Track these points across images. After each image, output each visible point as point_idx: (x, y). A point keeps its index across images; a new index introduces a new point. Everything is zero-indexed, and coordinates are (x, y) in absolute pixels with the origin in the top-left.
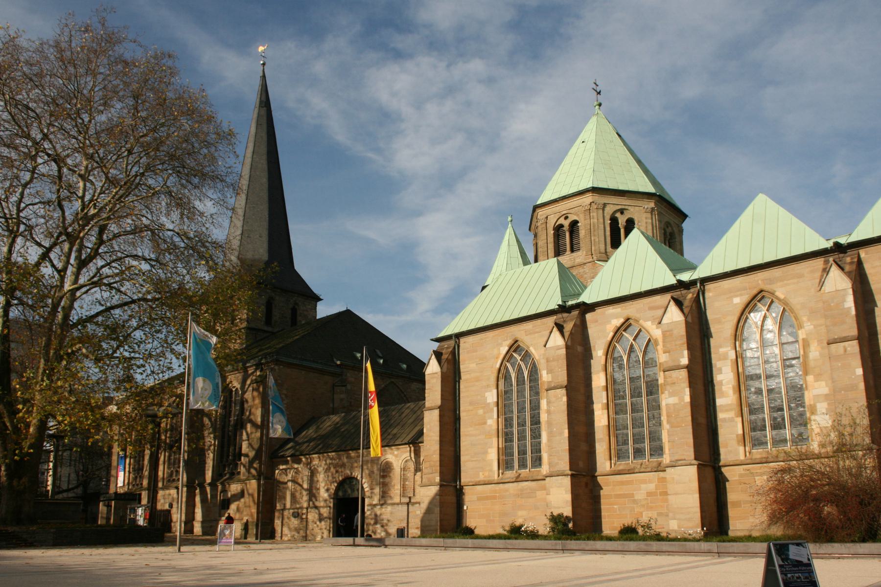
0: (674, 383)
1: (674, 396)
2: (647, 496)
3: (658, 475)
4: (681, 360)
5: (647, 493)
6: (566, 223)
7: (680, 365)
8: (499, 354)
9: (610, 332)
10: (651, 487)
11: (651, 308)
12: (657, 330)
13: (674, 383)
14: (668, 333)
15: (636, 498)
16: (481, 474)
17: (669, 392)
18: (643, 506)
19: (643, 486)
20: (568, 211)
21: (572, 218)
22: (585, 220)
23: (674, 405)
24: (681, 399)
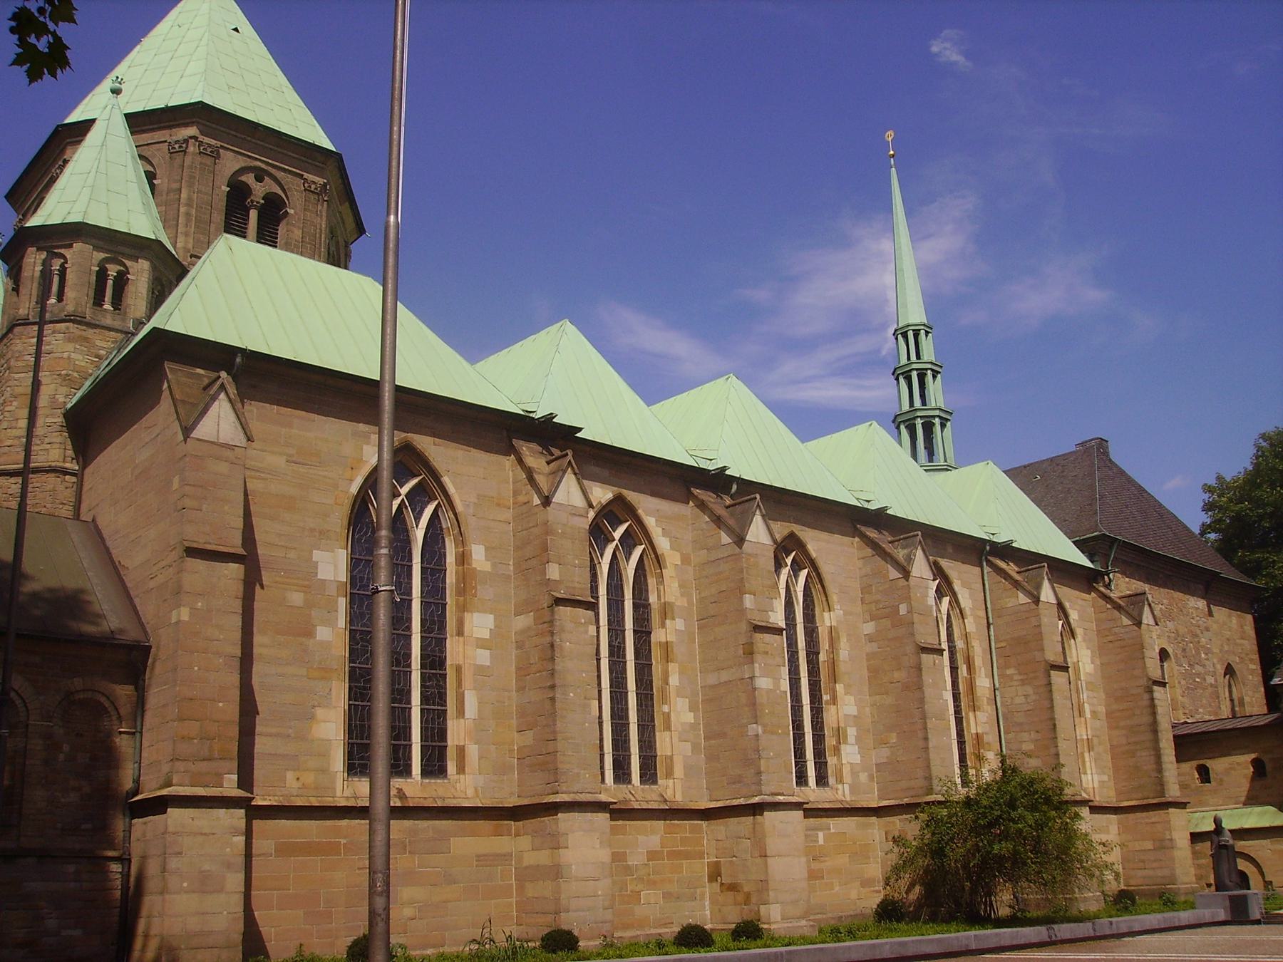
2: (648, 861)
6: (259, 190)
8: (360, 461)
12: (664, 538)
16: (290, 776)
18: (641, 879)
20: (269, 169)
21: (269, 186)
22: (305, 210)
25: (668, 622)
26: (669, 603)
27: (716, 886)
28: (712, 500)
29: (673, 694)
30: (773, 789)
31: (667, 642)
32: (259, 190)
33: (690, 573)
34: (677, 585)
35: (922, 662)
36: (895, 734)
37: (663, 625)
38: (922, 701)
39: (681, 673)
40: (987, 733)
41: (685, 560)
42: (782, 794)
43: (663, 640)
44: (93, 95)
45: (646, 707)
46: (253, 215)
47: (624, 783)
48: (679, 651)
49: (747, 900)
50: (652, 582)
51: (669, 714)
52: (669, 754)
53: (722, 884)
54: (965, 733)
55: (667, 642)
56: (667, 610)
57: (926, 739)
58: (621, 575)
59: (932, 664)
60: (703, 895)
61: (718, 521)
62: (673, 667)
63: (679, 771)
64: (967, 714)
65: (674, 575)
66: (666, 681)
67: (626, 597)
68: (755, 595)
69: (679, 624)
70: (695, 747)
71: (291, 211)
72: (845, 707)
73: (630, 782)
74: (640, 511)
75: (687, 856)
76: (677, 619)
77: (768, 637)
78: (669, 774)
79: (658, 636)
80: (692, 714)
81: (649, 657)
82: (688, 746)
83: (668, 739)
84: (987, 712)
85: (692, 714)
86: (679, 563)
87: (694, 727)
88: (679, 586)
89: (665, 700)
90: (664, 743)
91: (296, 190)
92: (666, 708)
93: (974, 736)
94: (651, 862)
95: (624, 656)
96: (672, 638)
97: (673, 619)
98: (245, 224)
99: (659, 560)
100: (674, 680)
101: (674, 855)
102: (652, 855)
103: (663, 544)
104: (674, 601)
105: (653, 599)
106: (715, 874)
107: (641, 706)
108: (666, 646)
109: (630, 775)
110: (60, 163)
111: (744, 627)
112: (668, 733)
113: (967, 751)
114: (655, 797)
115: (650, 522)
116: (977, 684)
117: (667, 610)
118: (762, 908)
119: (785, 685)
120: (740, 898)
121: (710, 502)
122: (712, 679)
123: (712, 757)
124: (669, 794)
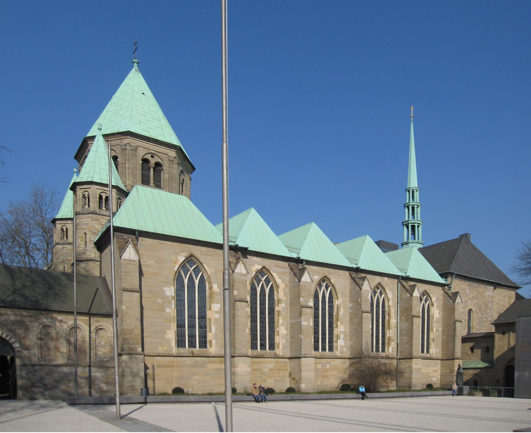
0: (306, 315)
1: (306, 321)
2: (269, 371)
3: (276, 360)
4: (309, 303)
5: (270, 369)
6: (153, 161)
7: (308, 305)
9: (253, 272)
10: (272, 366)
11: (277, 266)
12: (279, 280)
13: (306, 315)
14: (304, 287)
15: (264, 371)
17: (304, 319)
19: (267, 365)
21: (157, 159)
23: (306, 326)
24: (309, 323)
25: (279, 304)
26: (280, 299)
27: (290, 378)
28: (295, 267)
29: (280, 325)
30: (305, 353)
31: (279, 311)
32: (153, 161)
33: (288, 290)
34: (283, 293)
35: (363, 316)
36: (355, 337)
37: (278, 305)
38: (362, 328)
39: (283, 319)
40: (393, 337)
41: (286, 286)
42: (308, 354)
43: (278, 310)
44: (96, 124)
45: (272, 329)
46: (152, 170)
47: (264, 350)
48: (282, 313)
49: (297, 383)
50: (275, 292)
51: (279, 331)
52: (278, 342)
53: (292, 378)
54: (386, 336)
55: (279, 311)
56: (279, 301)
57: (362, 339)
58: (265, 291)
59: (367, 316)
60: (287, 381)
61: (295, 274)
62: (281, 318)
63: (281, 347)
64: (386, 331)
65: (282, 290)
66: (279, 322)
67: (266, 297)
68: (304, 297)
69: (283, 305)
70: (287, 340)
71: (164, 168)
72: (340, 329)
73: (266, 350)
74: (271, 272)
75: (282, 370)
76: (282, 304)
77: (307, 310)
78: (278, 347)
79: (277, 308)
80: (286, 331)
81: (274, 315)
82: (284, 340)
83: (278, 338)
84: (394, 330)
85: (286, 331)
86: (284, 287)
87: (286, 335)
88: (284, 294)
89: (278, 327)
90: (277, 339)
91: (166, 160)
92: (278, 329)
93: (388, 337)
94: (270, 372)
95: (265, 314)
96: (280, 309)
97: (281, 303)
98: (149, 172)
99: (277, 286)
100: (281, 321)
101: (277, 370)
102: (271, 369)
103: (279, 281)
104: (281, 298)
105: (275, 297)
106: (290, 375)
107: (270, 329)
108: (279, 311)
109: (266, 348)
110: (88, 151)
111: (300, 307)
112: (278, 336)
113: (386, 342)
114: (273, 354)
115: (275, 275)
116: (391, 321)
117: (279, 301)
118: (300, 384)
119: (312, 324)
120: (295, 381)
121: (294, 268)
122: (292, 321)
123: (291, 343)
124: (278, 353)
